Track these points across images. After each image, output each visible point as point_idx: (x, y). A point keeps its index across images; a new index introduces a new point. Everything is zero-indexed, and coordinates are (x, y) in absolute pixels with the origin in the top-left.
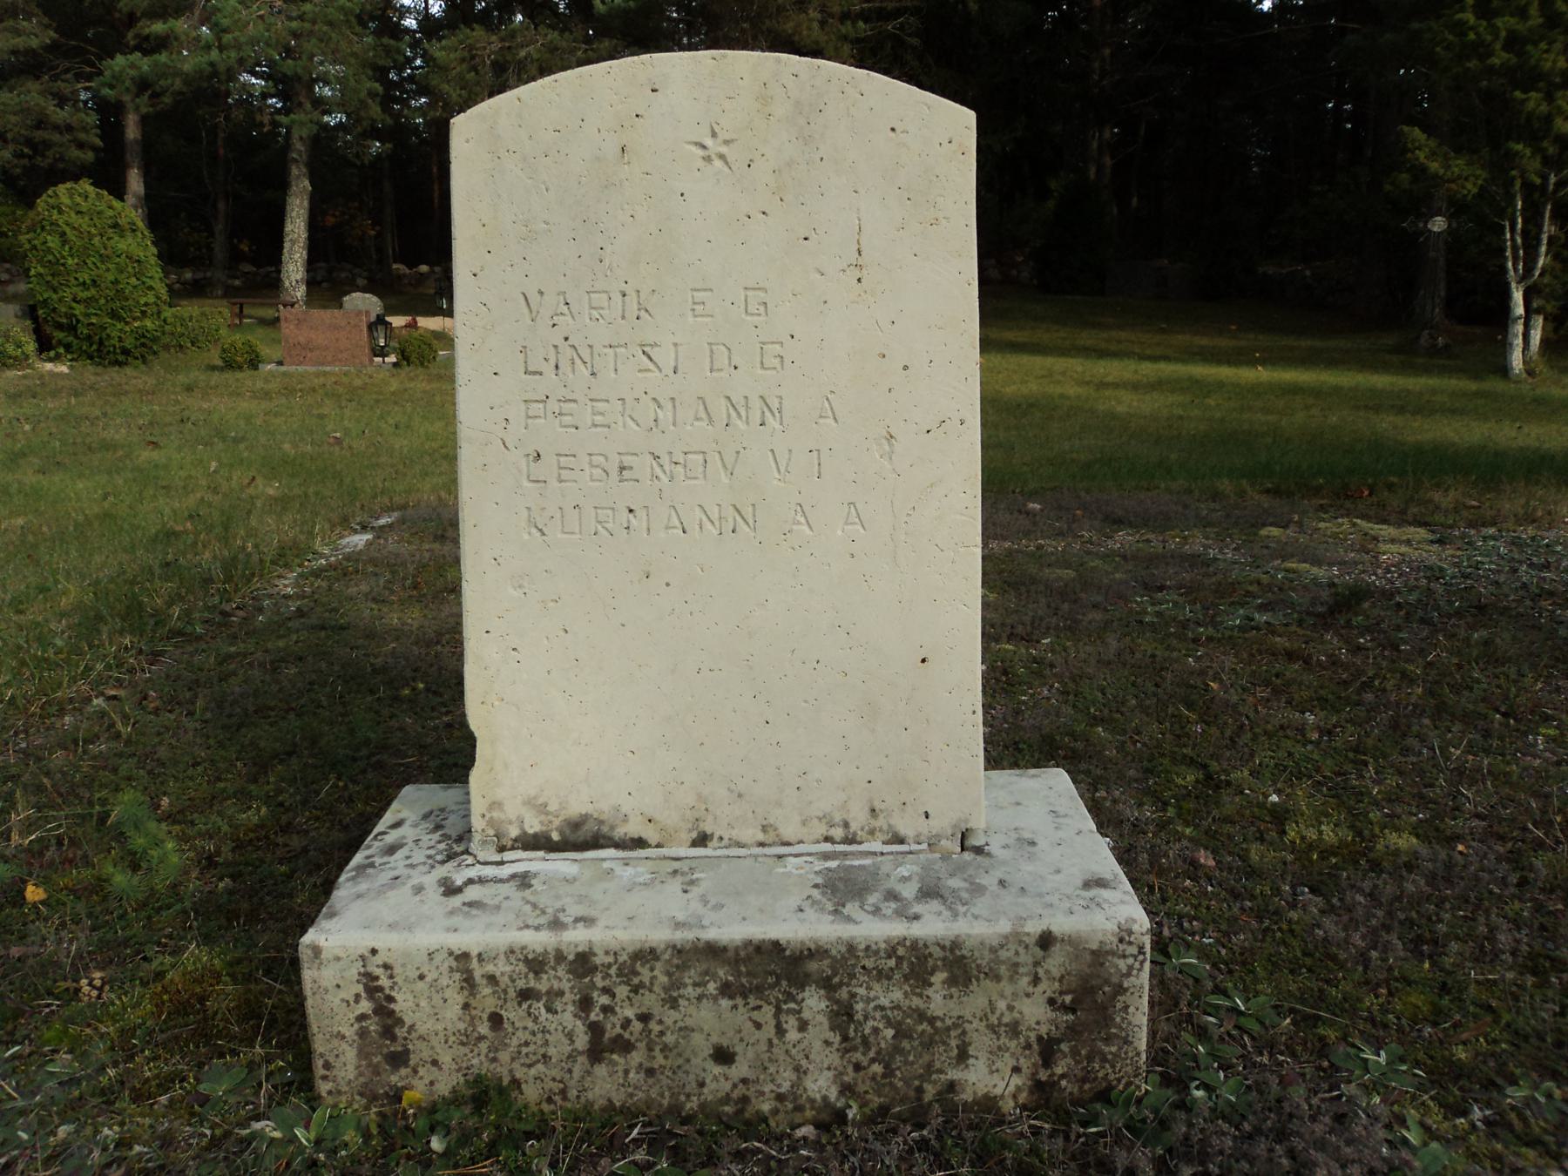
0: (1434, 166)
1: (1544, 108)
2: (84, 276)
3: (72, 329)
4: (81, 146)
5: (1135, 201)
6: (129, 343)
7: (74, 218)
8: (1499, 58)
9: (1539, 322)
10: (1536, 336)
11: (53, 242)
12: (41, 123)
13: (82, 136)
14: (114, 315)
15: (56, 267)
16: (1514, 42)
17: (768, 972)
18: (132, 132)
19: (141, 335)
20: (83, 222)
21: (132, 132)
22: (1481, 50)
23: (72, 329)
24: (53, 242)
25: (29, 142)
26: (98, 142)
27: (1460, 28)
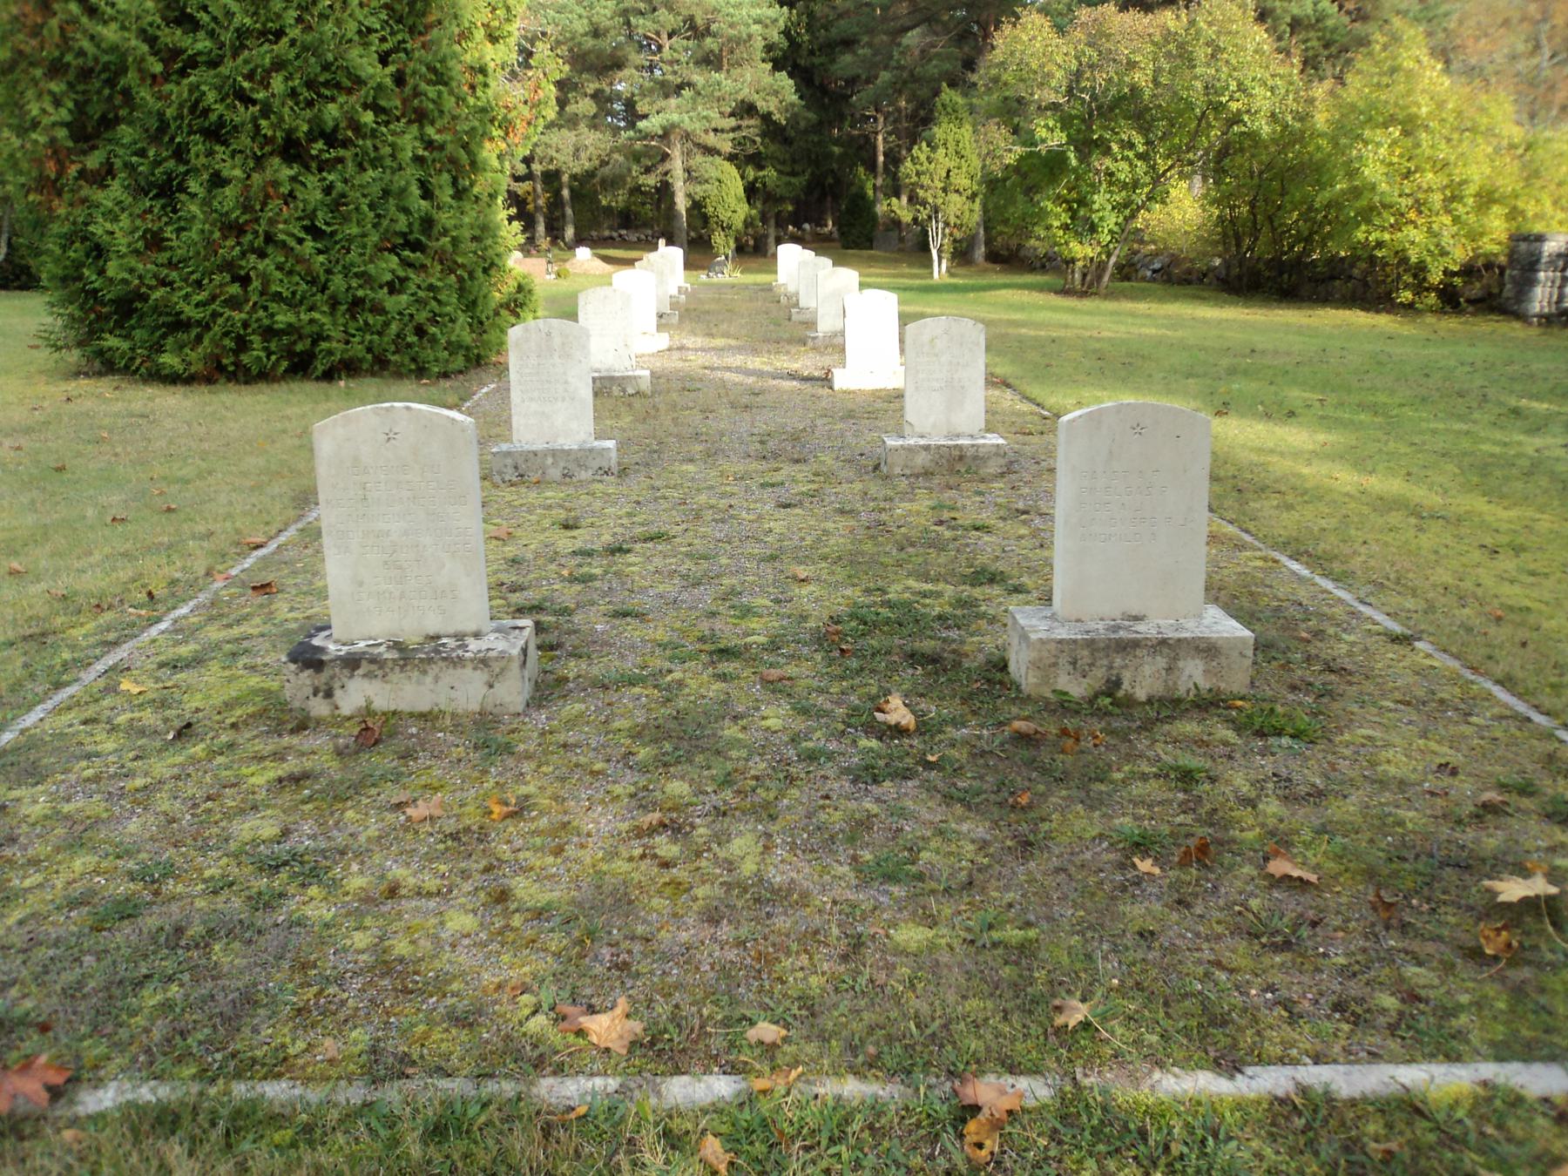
8: (915, 179)
22: (908, 176)
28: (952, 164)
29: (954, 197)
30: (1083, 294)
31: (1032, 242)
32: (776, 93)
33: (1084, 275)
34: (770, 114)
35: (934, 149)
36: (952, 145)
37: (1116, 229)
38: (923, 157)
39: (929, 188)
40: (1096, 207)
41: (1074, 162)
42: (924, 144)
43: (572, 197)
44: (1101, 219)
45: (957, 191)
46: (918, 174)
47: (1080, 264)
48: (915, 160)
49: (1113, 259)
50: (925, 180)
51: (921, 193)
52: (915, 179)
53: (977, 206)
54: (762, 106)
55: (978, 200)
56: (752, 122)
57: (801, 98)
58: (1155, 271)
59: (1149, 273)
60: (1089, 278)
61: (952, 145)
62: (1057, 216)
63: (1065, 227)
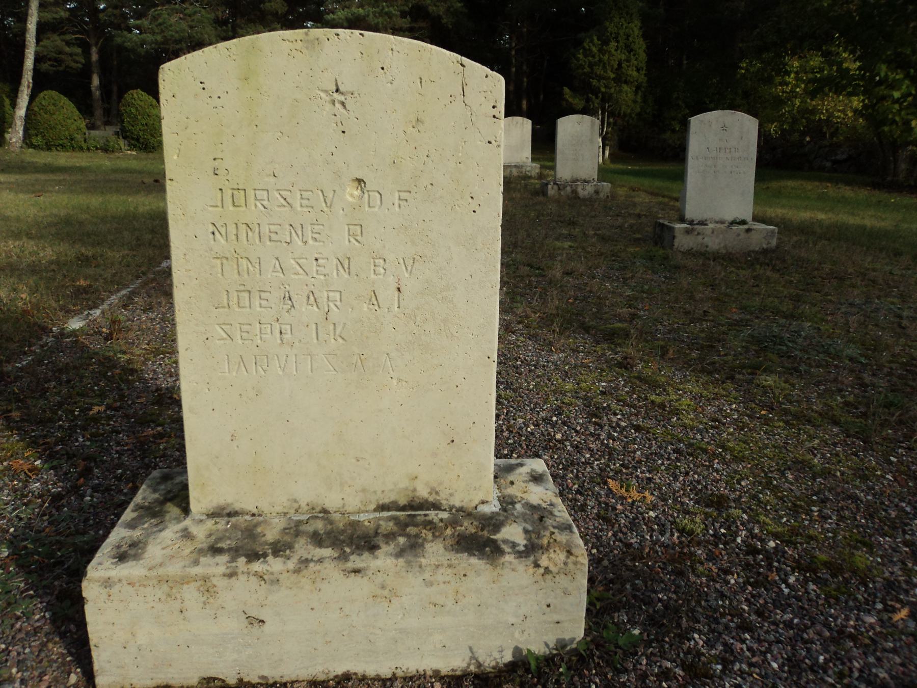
0: (570, 100)
1: (597, 84)
2: (144, 122)
3: (138, 140)
4: (77, 62)
5: (542, 97)
6: (156, 145)
8: (587, 69)
9: (608, 148)
10: (607, 153)
12: (60, 53)
13: (77, 58)
14: (152, 135)
16: (591, 65)
18: (95, 57)
20: (142, 104)
21: (95, 57)
22: (581, 67)
23: (138, 140)
24: (133, 110)
25: (56, 60)
26: (83, 61)
27: (578, 59)
28: (623, 57)
29: (625, 88)
31: (667, 135)
35: (606, 42)
38: (594, 49)
39: (600, 78)
42: (595, 38)
45: (626, 82)
46: (591, 65)
48: (588, 53)
50: (599, 70)
51: (594, 82)
52: (587, 69)
53: (639, 99)
54: (431, 9)
55: (640, 93)
56: (423, 25)
58: (835, 162)
59: (828, 164)
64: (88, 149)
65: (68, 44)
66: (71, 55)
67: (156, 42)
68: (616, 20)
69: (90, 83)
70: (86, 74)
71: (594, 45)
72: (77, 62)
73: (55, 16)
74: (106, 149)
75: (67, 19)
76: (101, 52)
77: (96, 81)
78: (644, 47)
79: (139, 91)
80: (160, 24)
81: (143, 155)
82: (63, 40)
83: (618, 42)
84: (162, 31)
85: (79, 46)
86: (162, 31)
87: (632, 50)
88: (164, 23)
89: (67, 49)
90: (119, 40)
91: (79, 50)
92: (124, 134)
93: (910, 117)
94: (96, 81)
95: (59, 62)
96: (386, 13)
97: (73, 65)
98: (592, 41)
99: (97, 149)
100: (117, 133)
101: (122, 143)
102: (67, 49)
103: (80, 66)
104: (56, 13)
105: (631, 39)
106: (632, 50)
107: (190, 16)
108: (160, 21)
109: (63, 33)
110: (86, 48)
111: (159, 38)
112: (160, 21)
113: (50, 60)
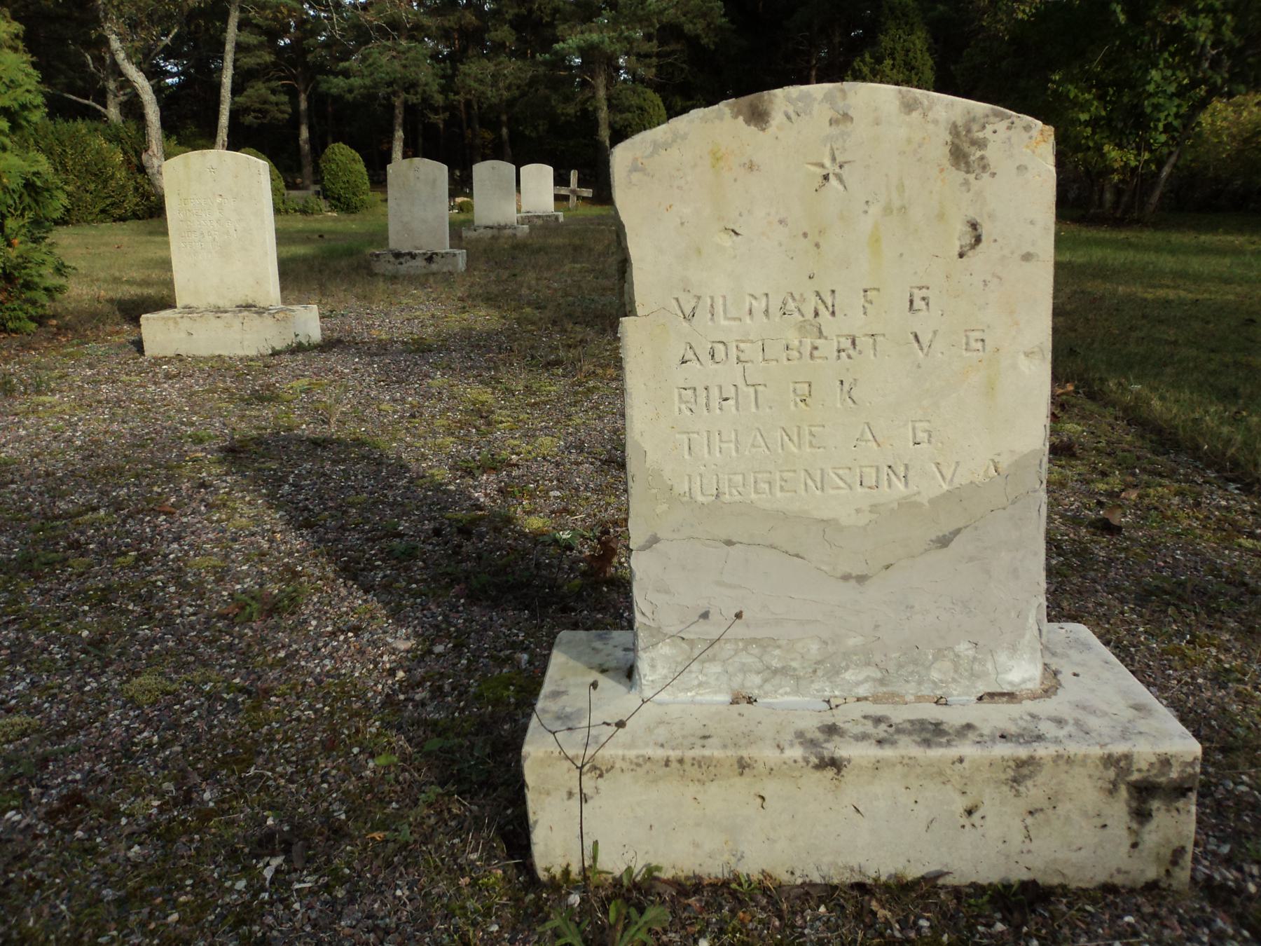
2: (345, 179)
3: (338, 199)
4: (283, 112)
7: (339, 157)
11: (334, 166)
12: (265, 102)
13: (282, 107)
14: (354, 194)
15: (336, 176)
17: (538, 217)
18: (303, 105)
19: (363, 201)
20: (343, 159)
21: (303, 105)
23: (338, 199)
24: (334, 166)
25: (260, 111)
26: (290, 110)
30: (1118, 223)
32: (704, 15)
33: (1118, 192)
34: (698, 37)
35: (879, 60)
36: (899, 57)
37: (1176, 123)
40: (1151, 88)
41: (1122, 18)
43: (510, 136)
44: (1157, 107)
47: (1116, 178)
49: (1166, 170)
54: (688, 27)
56: (679, 47)
57: (732, 21)
60: (1125, 199)
61: (899, 57)
62: (1084, 107)
63: (1094, 123)
64: (287, 212)
65: (274, 92)
66: (277, 104)
67: (365, 87)
68: (891, 32)
69: (298, 135)
70: (294, 124)
71: (865, 64)
72: (283, 112)
73: (259, 61)
74: (304, 212)
75: (272, 63)
76: (309, 99)
77: (304, 133)
78: (931, 62)
79: (341, 145)
80: (370, 65)
81: (344, 216)
82: (268, 88)
83: (894, 59)
84: (372, 74)
85: (285, 93)
86: (372, 74)
87: (913, 68)
88: (374, 63)
89: (273, 98)
90: (324, 87)
91: (285, 98)
92: (325, 194)
93: (1105, 141)
94: (304, 133)
95: (263, 112)
96: (626, 38)
97: (279, 116)
98: (863, 61)
99: (296, 211)
100: (318, 193)
101: (323, 204)
102: (273, 98)
103: (286, 116)
104: (260, 57)
105: (911, 54)
106: (913, 68)
107: (404, 53)
108: (371, 61)
109: (269, 80)
110: (293, 94)
111: (368, 82)
112: (371, 61)
113: (254, 111)
